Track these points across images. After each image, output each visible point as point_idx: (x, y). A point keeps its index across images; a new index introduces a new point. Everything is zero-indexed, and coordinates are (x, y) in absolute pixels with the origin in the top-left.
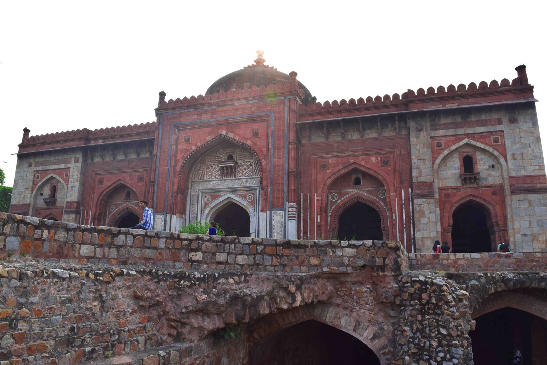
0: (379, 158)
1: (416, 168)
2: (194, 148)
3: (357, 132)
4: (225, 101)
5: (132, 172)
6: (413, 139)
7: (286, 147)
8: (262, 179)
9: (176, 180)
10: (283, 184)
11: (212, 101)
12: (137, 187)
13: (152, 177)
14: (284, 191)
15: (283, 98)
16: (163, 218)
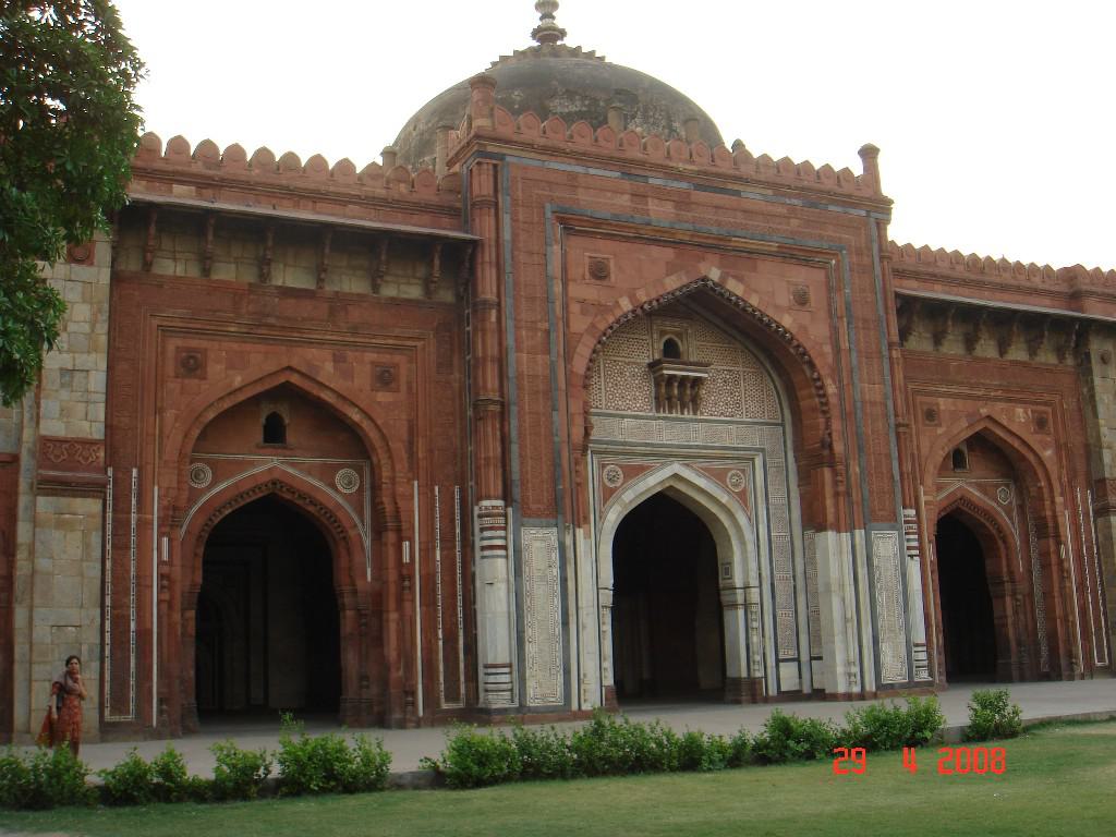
0: (1030, 413)
1: (1109, 448)
2: (626, 305)
3: (992, 343)
4: (718, 175)
5: (346, 344)
6: (1097, 381)
7: (884, 348)
8: (830, 434)
9: (576, 407)
10: (888, 456)
11: (681, 166)
12: (381, 411)
13: (491, 381)
14: (892, 477)
15: (863, 213)
16: (552, 535)
